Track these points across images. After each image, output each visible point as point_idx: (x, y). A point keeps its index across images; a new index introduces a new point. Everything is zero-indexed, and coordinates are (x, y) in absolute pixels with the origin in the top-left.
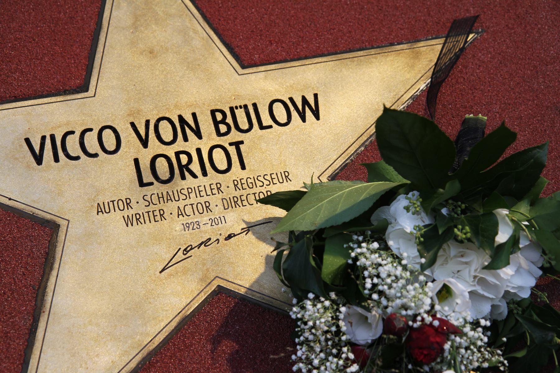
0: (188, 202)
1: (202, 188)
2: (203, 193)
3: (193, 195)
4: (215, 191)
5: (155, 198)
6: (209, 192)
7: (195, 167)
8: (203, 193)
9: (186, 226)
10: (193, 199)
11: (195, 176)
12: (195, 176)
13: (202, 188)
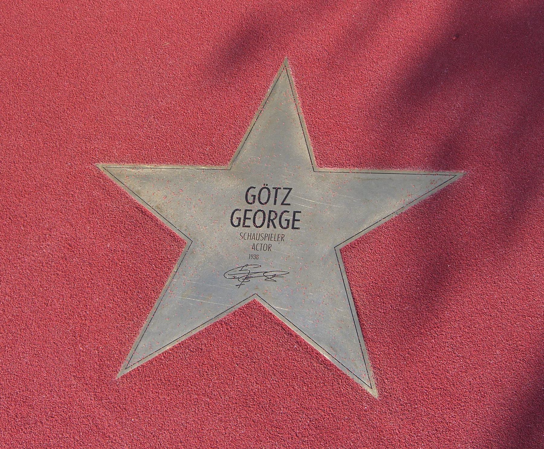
0: (264, 242)
2: (273, 239)
3: (267, 238)
4: (280, 239)
8: (273, 239)
10: (267, 242)
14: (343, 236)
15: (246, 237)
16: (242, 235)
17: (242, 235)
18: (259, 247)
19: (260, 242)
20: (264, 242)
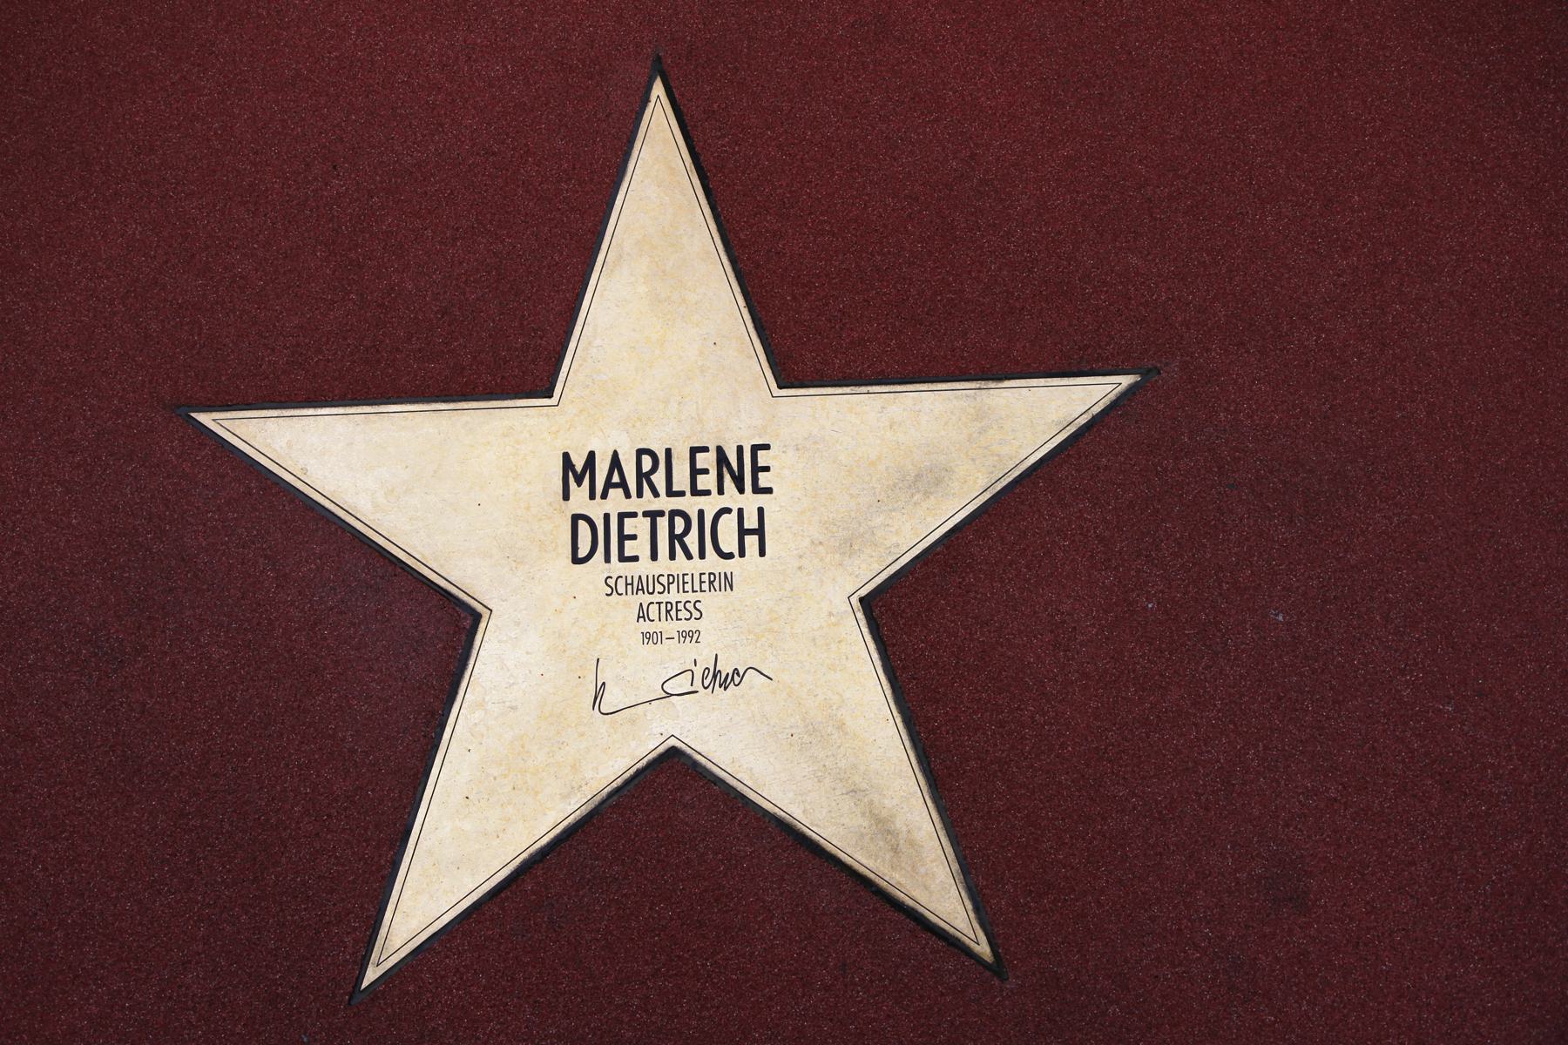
0: (664, 598)
1: (688, 579)
2: (688, 587)
3: (673, 587)
4: (705, 586)
5: (621, 582)
6: (697, 587)
7: (692, 540)
8: (688, 587)
9: (647, 637)
10: (673, 596)
11: (689, 556)
12: (689, 556)
13: (688, 579)
14: (871, 570)
15: (621, 589)
16: (611, 582)
17: (611, 582)
18: (654, 609)
19: (656, 598)
20: (664, 598)
